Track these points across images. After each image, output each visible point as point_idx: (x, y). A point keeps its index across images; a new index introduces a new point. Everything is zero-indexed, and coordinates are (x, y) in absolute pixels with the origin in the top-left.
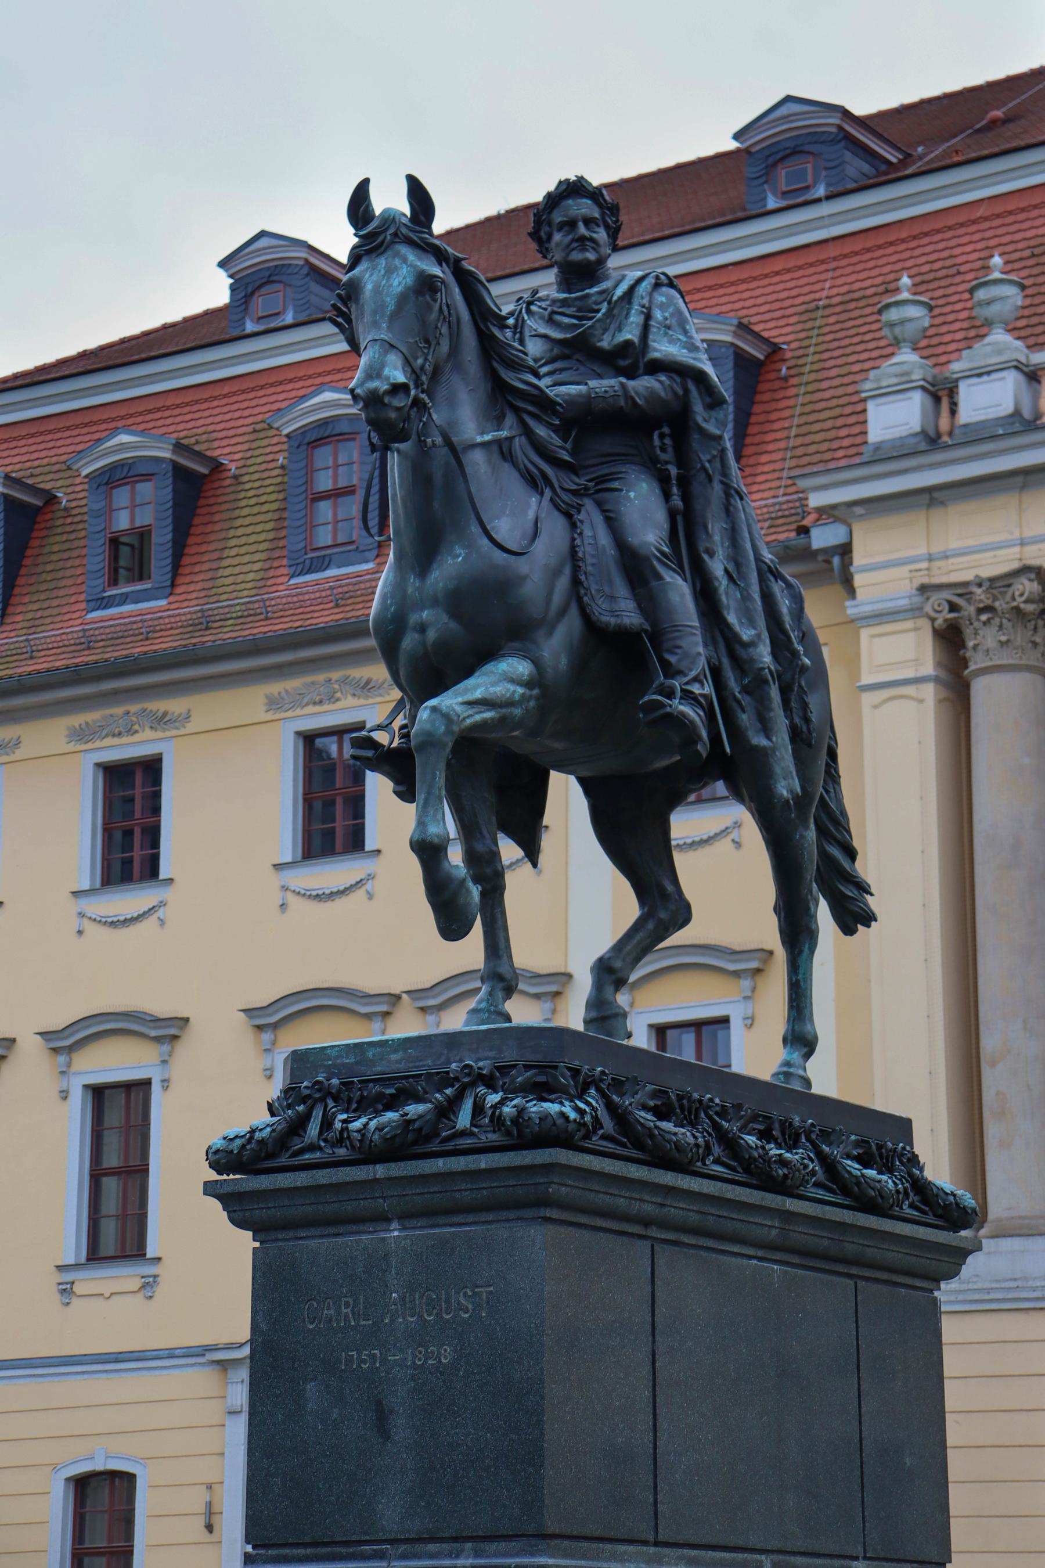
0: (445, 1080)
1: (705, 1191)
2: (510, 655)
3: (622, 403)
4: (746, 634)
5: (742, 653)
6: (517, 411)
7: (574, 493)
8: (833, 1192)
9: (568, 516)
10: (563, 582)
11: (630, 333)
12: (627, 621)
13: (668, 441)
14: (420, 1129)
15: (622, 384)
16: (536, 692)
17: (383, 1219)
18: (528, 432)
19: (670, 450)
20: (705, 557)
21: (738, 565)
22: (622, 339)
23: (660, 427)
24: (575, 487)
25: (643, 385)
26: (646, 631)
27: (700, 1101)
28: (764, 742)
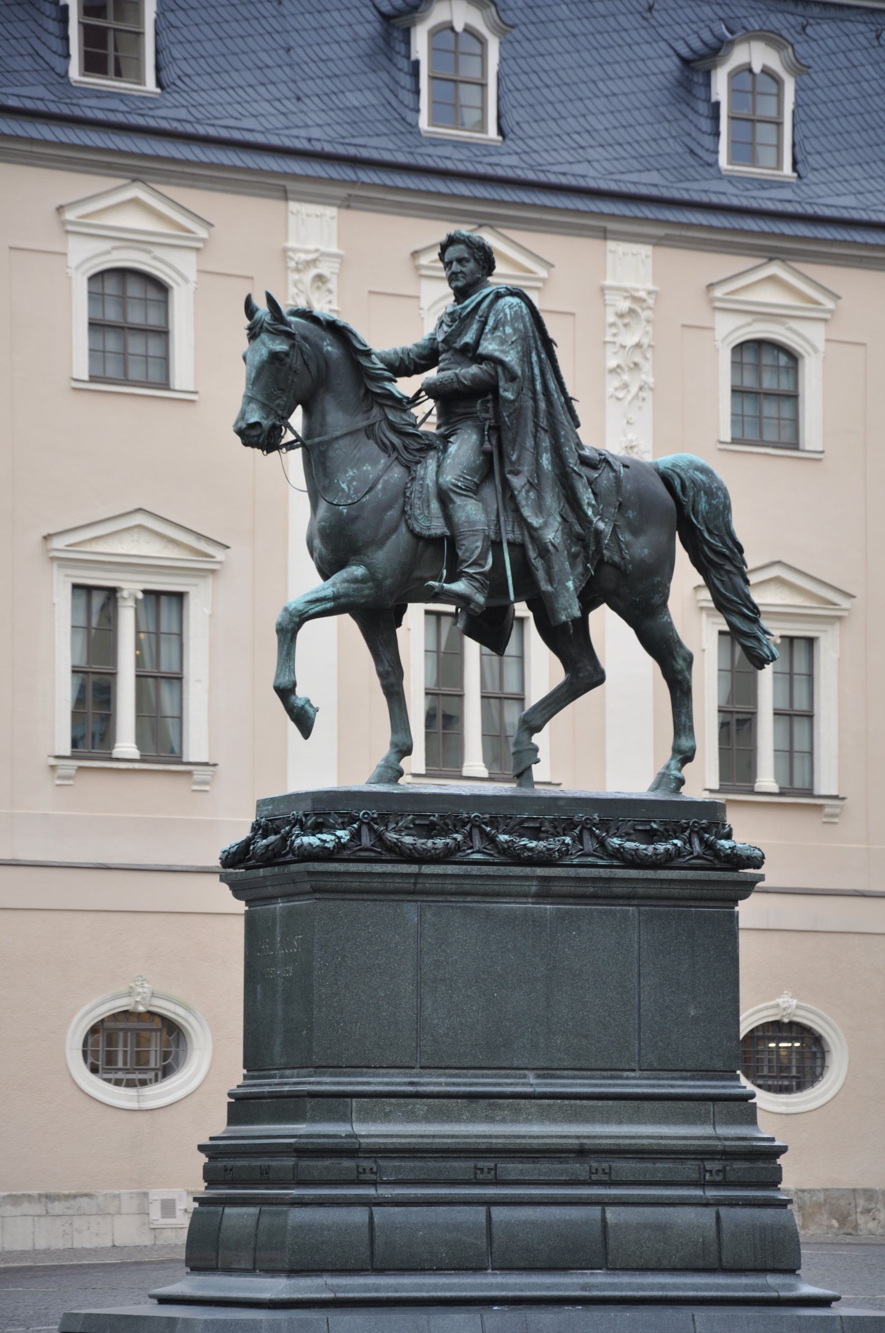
0: (288, 822)
1: (450, 872)
2: (354, 565)
3: (456, 386)
4: (536, 522)
5: (535, 534)
6: (382, 406)
7: (418, 450)
8: (602, 858)
9: (408, 468)
10: (393, 514)
11: (469, 338)
12: (433, 532)
13: (490, 405)
14: (273, 850)
15: (456, 374)
16: (370, 584)
17: (271, 898)
18: (387, 418)
19: (491, 410)
20: (509, 476)
21: (538, 477)
22: (463, 342)
23: (487, 395)
24: (418, 446)
25: (474, 369)
26: (447, 536)
27: (469, 818)
28: (549, 588)
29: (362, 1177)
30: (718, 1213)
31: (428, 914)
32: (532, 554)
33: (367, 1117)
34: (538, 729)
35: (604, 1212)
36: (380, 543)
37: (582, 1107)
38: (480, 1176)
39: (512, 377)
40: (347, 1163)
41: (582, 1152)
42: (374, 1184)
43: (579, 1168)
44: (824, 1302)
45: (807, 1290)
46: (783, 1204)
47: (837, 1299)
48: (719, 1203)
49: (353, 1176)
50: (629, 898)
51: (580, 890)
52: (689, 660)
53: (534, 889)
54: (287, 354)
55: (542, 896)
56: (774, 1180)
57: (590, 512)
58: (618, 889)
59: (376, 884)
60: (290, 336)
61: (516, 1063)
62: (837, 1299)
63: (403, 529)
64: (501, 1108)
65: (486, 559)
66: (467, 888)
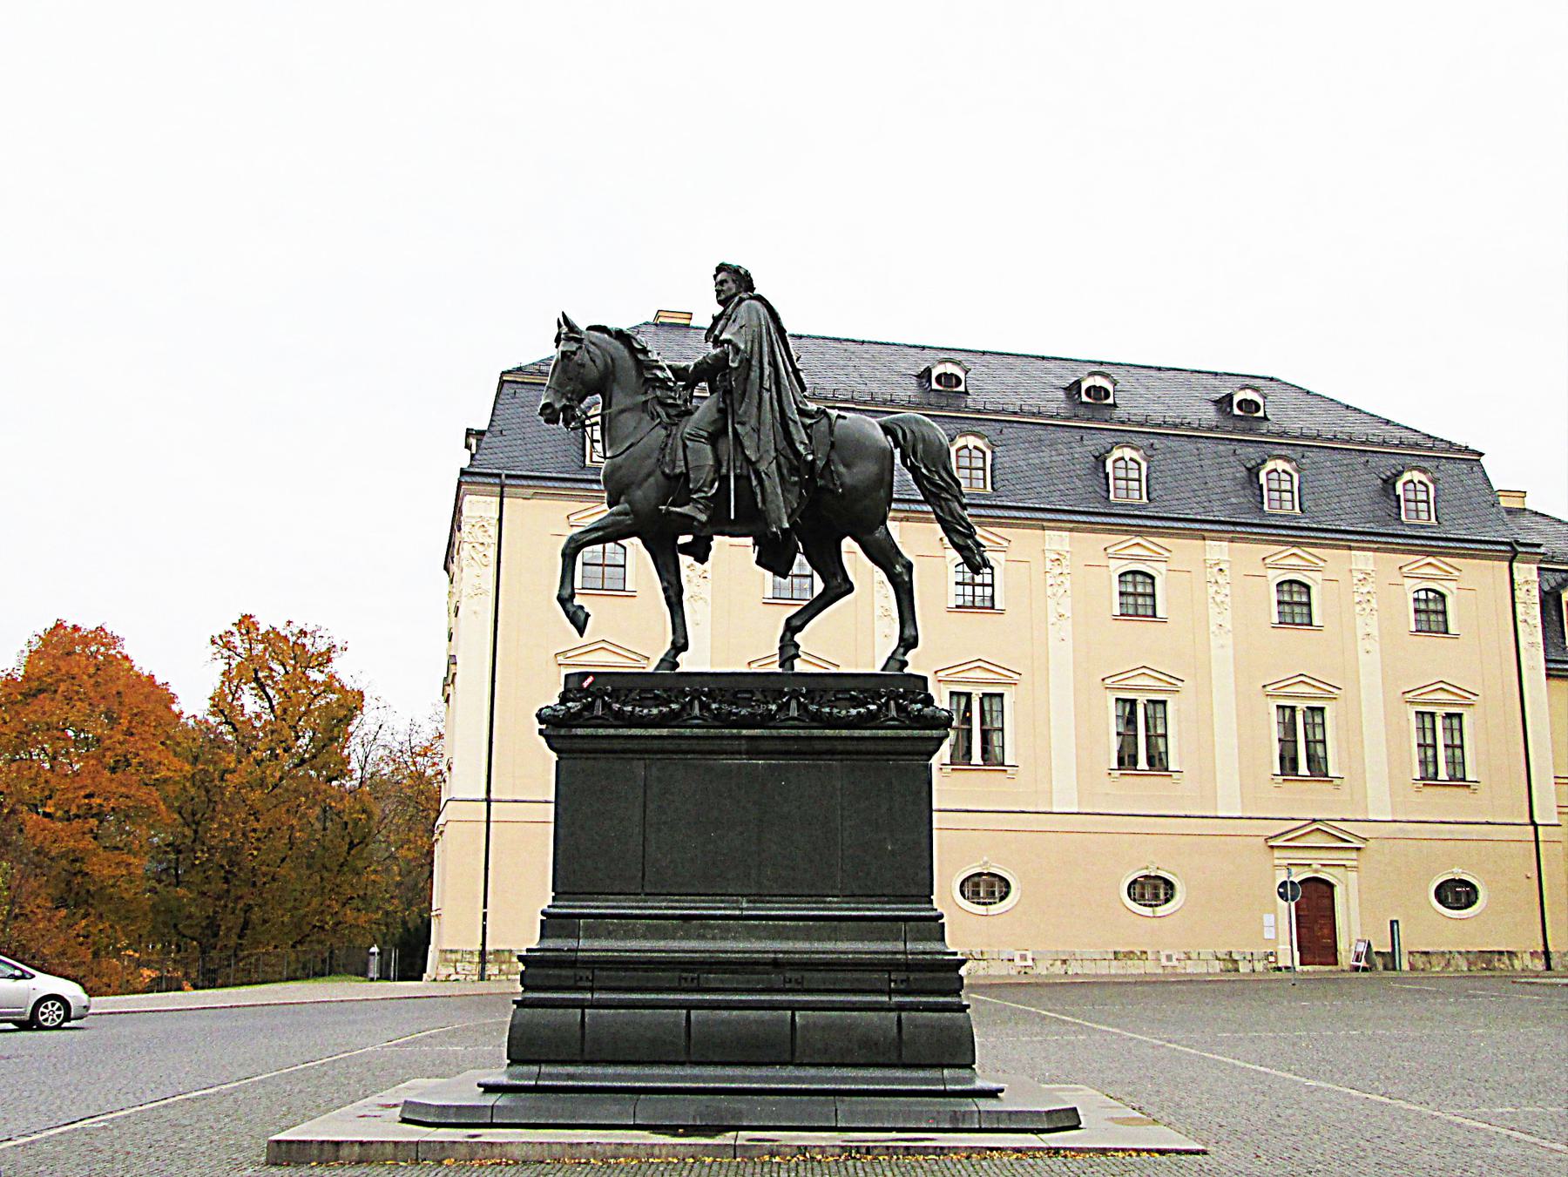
29: (580, 984)
30: (899, 1018)
31: (654, 770)
32: (754, 483)
33: (592, 934)
34: (800, 628)
35: (793, 1016)
36: (640, 486)
37: (784, 927)
38: (684, 985)
39: (737, 350)
40: (570, 972)
41: (776, 964)
42: (592, 990)
43: (775, 978)
44: (993, 1094)
45: (979, 1084)
46: (964, 1008)
47: (1002, 1090)
48: (901, 1007)
49: (571, 983)
50: (832, 752)
51: (784, 748)
52: (909, 567)
53: (744, 748)
54: (574, 353)
55: (753, 753)
56: (957, 987)
57: (801, 448)
58: (818, 746)
59: (605, 745)
60: (579, 341)
61: (730, 891)
62: (1002, 1090)
63: (658, 473)
64: (711, 927)
65: (711, 487)
66: (684, 747)
